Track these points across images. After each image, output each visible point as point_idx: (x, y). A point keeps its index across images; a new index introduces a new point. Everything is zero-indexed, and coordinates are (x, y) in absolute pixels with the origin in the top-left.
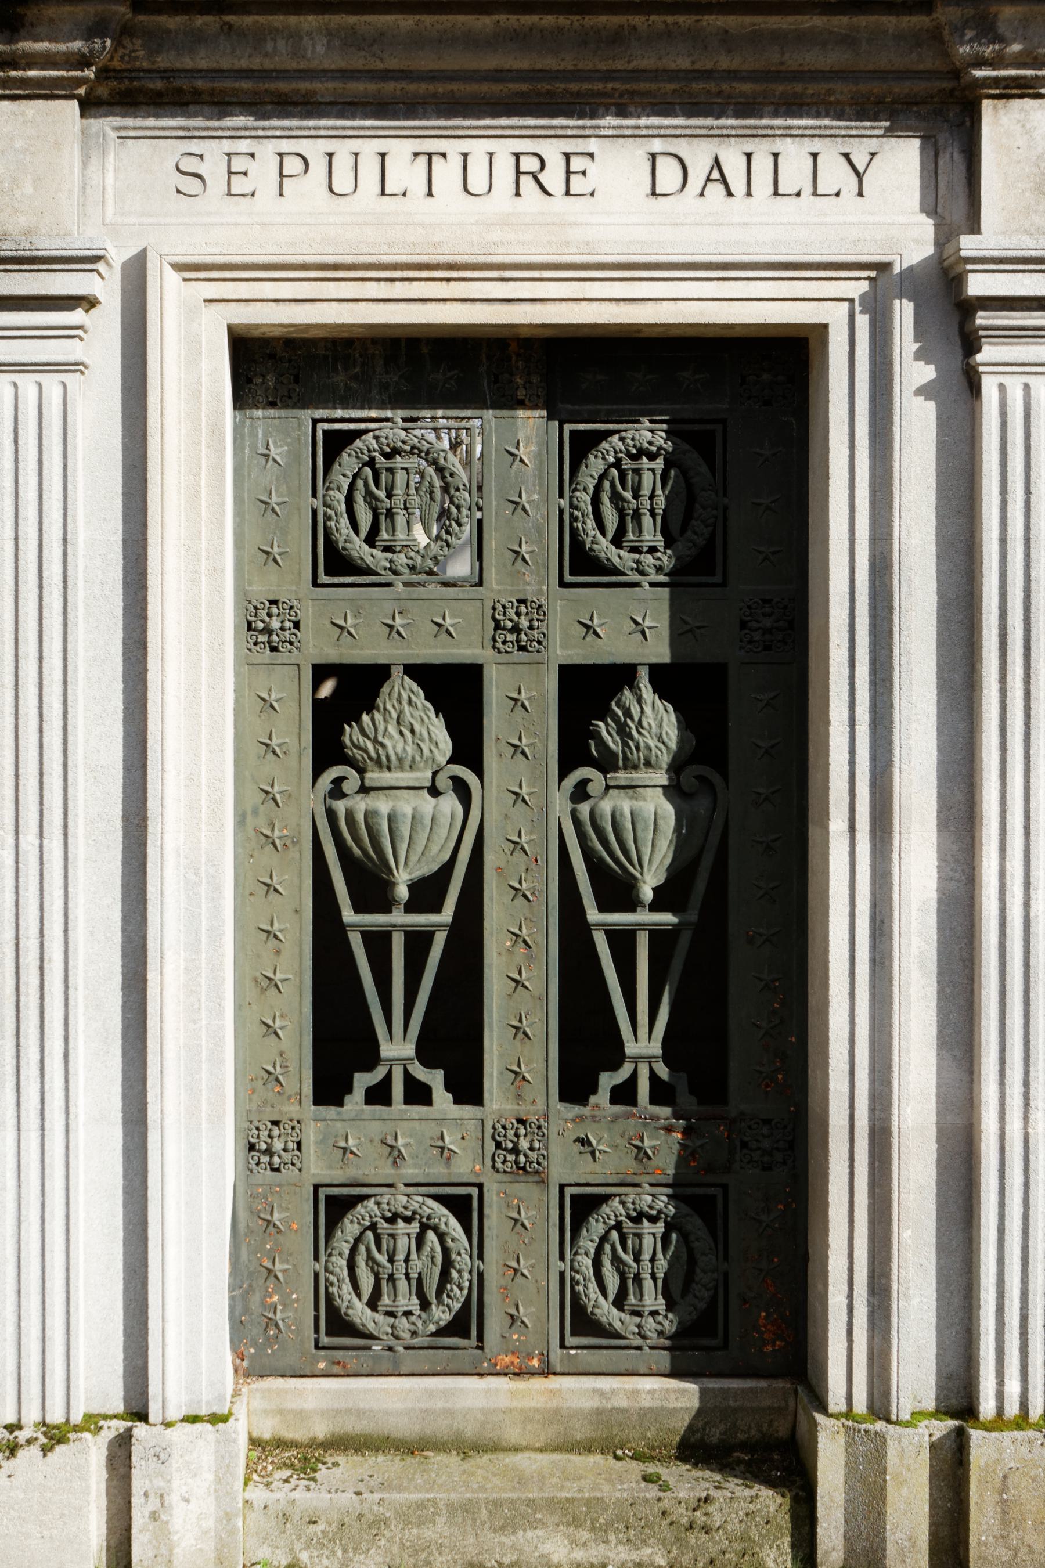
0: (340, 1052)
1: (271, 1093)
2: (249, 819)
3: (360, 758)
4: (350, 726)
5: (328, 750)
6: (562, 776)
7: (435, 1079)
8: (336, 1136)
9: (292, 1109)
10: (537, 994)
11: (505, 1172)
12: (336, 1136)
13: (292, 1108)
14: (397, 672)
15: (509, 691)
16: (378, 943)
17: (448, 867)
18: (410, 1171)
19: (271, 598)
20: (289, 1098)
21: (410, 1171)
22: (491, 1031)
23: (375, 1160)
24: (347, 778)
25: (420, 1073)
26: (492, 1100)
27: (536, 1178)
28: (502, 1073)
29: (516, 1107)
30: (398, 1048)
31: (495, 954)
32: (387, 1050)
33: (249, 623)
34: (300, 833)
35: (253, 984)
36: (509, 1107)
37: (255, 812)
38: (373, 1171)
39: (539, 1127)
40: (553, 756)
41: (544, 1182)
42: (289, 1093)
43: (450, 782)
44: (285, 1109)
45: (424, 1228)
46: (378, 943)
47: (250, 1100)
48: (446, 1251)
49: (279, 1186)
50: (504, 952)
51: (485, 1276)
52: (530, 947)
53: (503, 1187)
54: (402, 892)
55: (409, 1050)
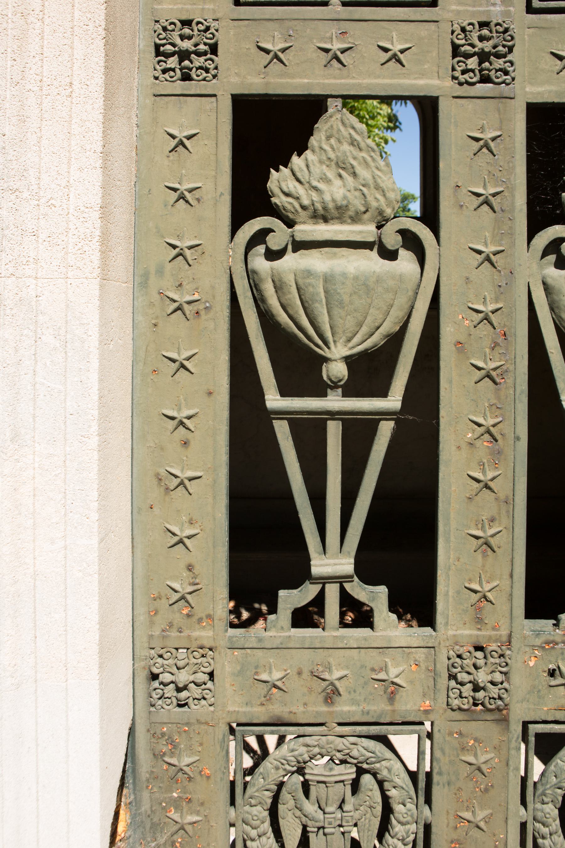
0: (263, 558)
1: (177, 615)
2: (153, 280)
3: (289, 207)
4: (277, 170)
5: (250, 199)
6: (533, 231)
7: (376, 597)
8: (257, 667)
9: (205, 635)
10: (502, 496)
11: (460, 709)
12: (257, 667)
13: (203, 633)
14: (333, 105)
15: (472, 130)
16: (310, 431)
17: (396, 340)
18: (346, 708)
19: (184, 18)
20: (200, 620)
21: (345, 708)
22: (448, 541)
23: (304, 695)
24: (274, 231)
25: (359, 591)
26: (447, 624)
27: (496, 716)
28: (458, 592)
29: (476, 632)
30: (333, 561)
31: (454, 448)
32: (320, 566)
33: (157, 47)
34: (214, 297)
35: (155, 481)
36: (467, 632)
37: (160, 271)
38: (301, 709)
39: (502, 656)
40: (521, 210)
41: (504, 721)
42: (200, 615)
43: (399, 238)
44: (196, 634)
45: (360, 772)
46: (310, 431)
47: (152, 623)
48: (386, 799)
49: (187, 724)
50: (464, 446)
51: (434, 829)
52: (496, 441)
53: (456, 727)
54: (338, 370)
55: (346, 565)
